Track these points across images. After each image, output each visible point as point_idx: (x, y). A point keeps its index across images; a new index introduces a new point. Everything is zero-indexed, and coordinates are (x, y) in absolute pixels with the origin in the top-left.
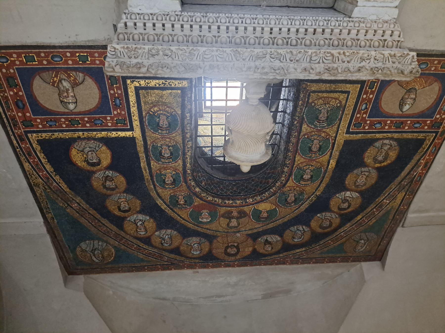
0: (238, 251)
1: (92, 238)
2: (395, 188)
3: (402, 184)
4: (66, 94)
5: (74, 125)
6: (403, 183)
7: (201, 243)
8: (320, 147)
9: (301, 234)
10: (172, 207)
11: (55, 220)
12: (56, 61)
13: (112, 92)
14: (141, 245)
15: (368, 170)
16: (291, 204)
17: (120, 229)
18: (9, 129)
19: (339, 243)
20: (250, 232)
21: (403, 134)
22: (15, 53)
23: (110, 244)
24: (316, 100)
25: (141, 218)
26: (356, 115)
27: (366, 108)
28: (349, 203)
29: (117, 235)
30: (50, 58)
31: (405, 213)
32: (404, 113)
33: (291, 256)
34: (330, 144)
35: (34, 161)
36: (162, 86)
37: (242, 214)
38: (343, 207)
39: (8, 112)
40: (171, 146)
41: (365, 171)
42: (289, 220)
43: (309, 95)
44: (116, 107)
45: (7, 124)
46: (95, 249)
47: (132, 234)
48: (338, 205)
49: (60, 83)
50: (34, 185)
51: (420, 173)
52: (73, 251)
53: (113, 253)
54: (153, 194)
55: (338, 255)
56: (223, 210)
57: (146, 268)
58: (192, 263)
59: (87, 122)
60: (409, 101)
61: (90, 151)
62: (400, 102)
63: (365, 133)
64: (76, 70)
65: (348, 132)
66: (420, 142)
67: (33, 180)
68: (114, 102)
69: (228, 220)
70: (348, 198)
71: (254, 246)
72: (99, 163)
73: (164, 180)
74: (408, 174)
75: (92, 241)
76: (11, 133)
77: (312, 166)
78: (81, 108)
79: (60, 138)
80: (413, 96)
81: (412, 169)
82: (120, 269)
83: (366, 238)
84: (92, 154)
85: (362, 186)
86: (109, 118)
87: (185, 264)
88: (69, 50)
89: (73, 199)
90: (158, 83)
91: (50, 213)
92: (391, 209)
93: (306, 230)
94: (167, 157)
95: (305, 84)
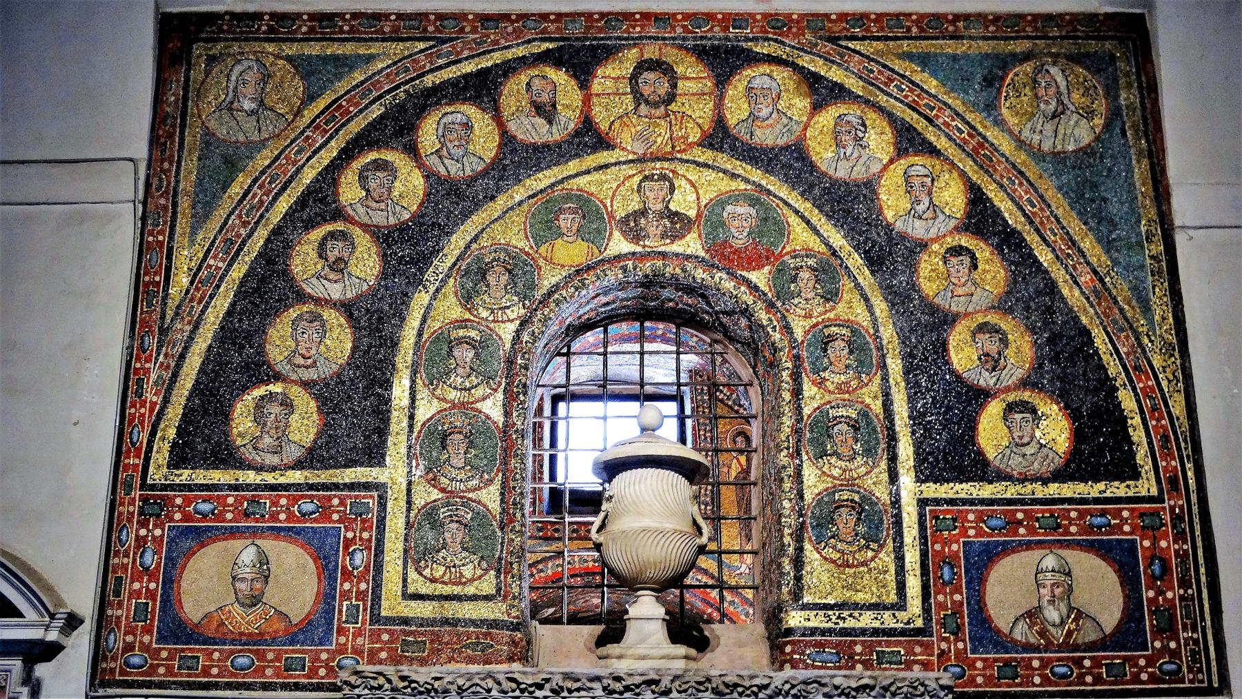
0: (634, 78)
1: (1058, 158)
2: (203, 312)
3: (189, 323)
4: (1058, 591)
5: (1052, 516)
6: (188, 328)
7: (750, 121)
8: (444, 448)
9: (448, 144)
10: (832, 259)
11: (1143, 229)
12: (1064, 666)
13: (957, 597)
14: (920, 124)
15: (300, 371)
16: (494, 260)
17: (979, 188)
18: (1195, 509)
19: (321, 104)
20: (604, 157)
21: (233, 482)
22: (1143, 683)
23: (1011, 132)
24: (480, 577)
25: (918, 223)
26: (371, 536)
27: (352, 554)
28: (327, 260)
29: (986, 168)
30: (1076, 671)
31: (144, 219)
32: (249, 542)
33: (466, 53)
34: (421, 454)
35: (1158, 420)
36: (845, 614)
37: (632, 226)
38: (341, 244)
39: (1186, 551)
40: (830, 455)
41: (307, 367)
42: (493, 198)
43: (499, 590)
44: (952, 562)
45: (1196, 520)
46: (1053, 117)
47: (946, 167)
48: (357, 254)
49: (1065, 616)
50: (1174, 349)
51: (148, 360)
52: (1115, 114)
53: (1006, 100)
54: (880, 307)
55: (314, 49)
56: (692, 244)
57: (914, 30)
58: (776, 41)
59: (1020, 523)
60: (246, 572)
61: (1023, 445)
62: (269, 569)
63: (336, 486)
64: (1028, 647)
65: (380, 487)
66: (179, 458)
67: (1174, 362)
68: (955, 574)
69: (672, 207)
70: (332, 276)
71: (587, 101)
72: (1010, 408)
73: (851, 352)
74: (182, 357)
75: (1059, 147)
76: (1194, 498)
77: (455, 388)
78: (1029, 558)
79: (1087, 483)
80: (241, 586)
81: (175, 375)
82: (992, 28)
83: (240, 116)
84: (1021, 438)
85: (300, 317)
86: (972, 532)
87: (796, 35)
88: (1035, 689)
89: (1088, 299)
90: (854, 618)
91: (1152, 257)
92: (193, 233)
93: (434, 159)
94: (841, 422)
95: (514, 618)
